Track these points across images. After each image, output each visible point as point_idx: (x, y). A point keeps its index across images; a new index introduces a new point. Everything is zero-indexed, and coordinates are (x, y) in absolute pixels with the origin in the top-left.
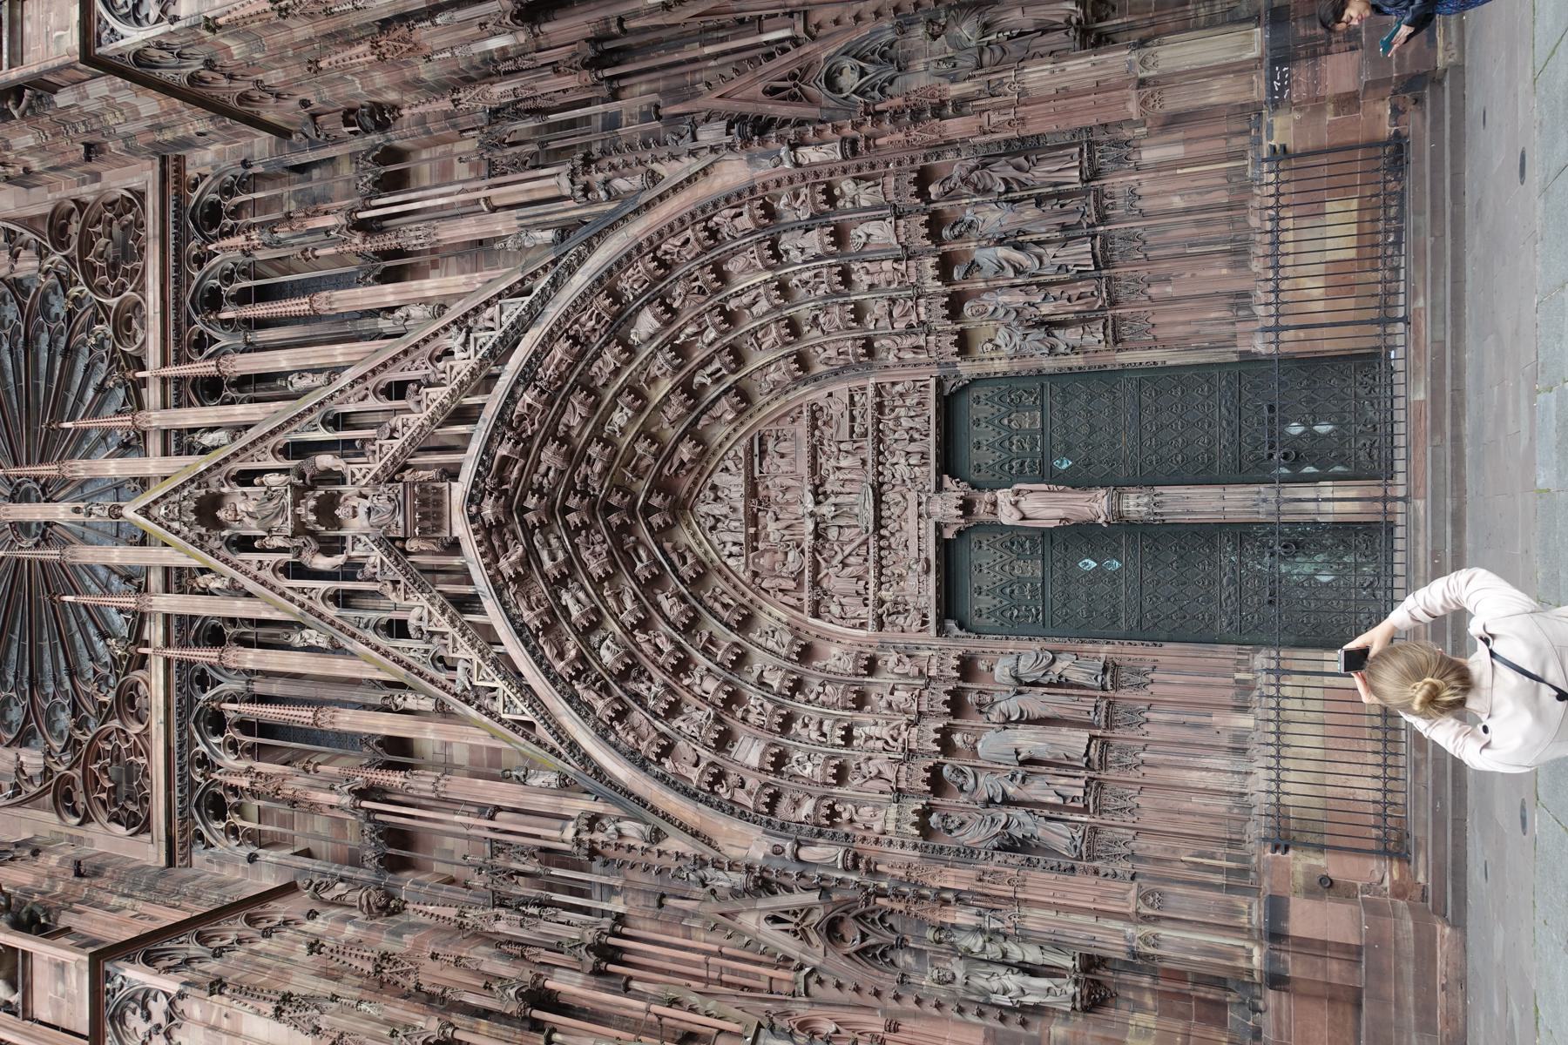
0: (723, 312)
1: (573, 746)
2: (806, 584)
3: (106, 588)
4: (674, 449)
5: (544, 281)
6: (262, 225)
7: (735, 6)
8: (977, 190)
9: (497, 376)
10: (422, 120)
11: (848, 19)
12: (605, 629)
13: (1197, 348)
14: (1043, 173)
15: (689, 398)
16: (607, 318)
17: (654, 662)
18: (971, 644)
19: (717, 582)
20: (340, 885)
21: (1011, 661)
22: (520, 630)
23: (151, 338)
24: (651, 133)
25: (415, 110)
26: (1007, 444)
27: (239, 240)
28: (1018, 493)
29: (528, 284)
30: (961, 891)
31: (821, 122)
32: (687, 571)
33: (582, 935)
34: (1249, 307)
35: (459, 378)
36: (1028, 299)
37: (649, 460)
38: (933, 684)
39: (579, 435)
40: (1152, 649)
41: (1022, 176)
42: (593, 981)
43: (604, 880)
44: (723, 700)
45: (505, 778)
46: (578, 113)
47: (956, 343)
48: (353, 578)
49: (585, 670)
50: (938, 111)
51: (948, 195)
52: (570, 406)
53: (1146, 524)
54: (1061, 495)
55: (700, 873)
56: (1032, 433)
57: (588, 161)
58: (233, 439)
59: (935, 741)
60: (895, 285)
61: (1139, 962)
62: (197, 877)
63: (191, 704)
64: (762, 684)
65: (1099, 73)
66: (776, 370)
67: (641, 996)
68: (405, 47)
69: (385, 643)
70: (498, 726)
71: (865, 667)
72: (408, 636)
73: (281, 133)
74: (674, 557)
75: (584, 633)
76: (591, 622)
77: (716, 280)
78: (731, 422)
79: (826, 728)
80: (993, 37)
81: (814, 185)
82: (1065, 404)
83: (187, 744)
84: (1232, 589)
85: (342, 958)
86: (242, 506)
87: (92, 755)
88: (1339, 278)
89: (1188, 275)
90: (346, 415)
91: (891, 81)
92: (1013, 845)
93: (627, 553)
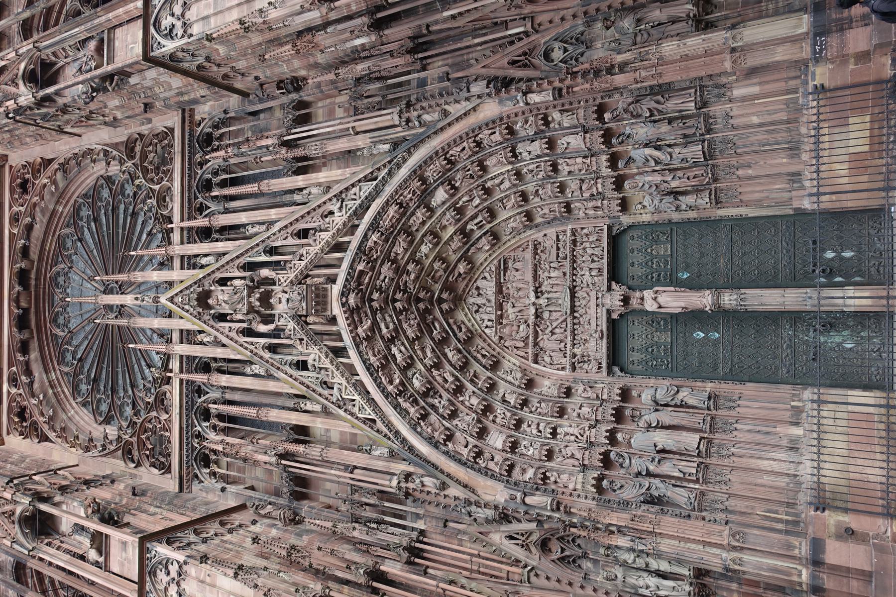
0: (484, 188)
1: (397, 433)
2: (531, 344)
3: (150, 341)
4: (456, 266)
5: (384, 172)
6: (233, 145)
7: (492, 15)
8: (633, 116)
9: (358, 226)
10: (319, 85)
11: (557, 20)
12: (416, 368)
13: (768, 206)
14: (672, 105)
15: (464, 238)
17: (443, 387)
18: (627, 381)
19: (479, 342)
20: (269, 507)
21: (652, 391)
22: (369, 367)
23: (176, 206)
24: (444, 88)
25: (315, 80)
26: (650, 263)
27: (222, 153)
28: (656, 292)
29: (375, 174)
30: (621, 526)
31: (541, 79)
32: (462, 336)
33: (401, 541)
34: (800, 181)
36: (663, 178)
37: (441, 272)
38: (605, 404)
39: (402, 258)
40: (739, 386)
41: (660, 107)
42: (406, 567)
43: (413, 510)
44: (482, 410)
45: (359, 450)
47: (619, 205)
48: (279, 337)
49: (404, 391)
50: (610, 71)
51: (615, 119)
53: (735, 311)
54: (683, 294)
55: (468, 508)
56: (665, 257)
57: (409, 105)
58: (217, 261)
59: (606, 437)
60: (583, 172)
61: (730, 574)
62: (194, 498)
63: (193, 404)
64: (504, 401)
65: (707, 45)
66: (514, 221)
67: (433, 578)
68: (310, 45)
69: (295, 373)
70: (356, 421)
71: (565, 393)
72: (307, 369)
73: (244, 94)
74: (455, 328)
75: (404, 370)
76: (408, 363)
77: (480, 170)
78: (488, 251)
79: (541, 428)
80: (643, 27)
81: (537, 115)
82: (685, 239)
83: (190, 426)
84: (789, 351)
85: (270, 547)
86: (221, 297)
87: (142, 430)
88: (858, 163)
89: (762, 163)
90: (276, 247)
91: (582, 54)
92: (652, 500)
93: (428, 325)
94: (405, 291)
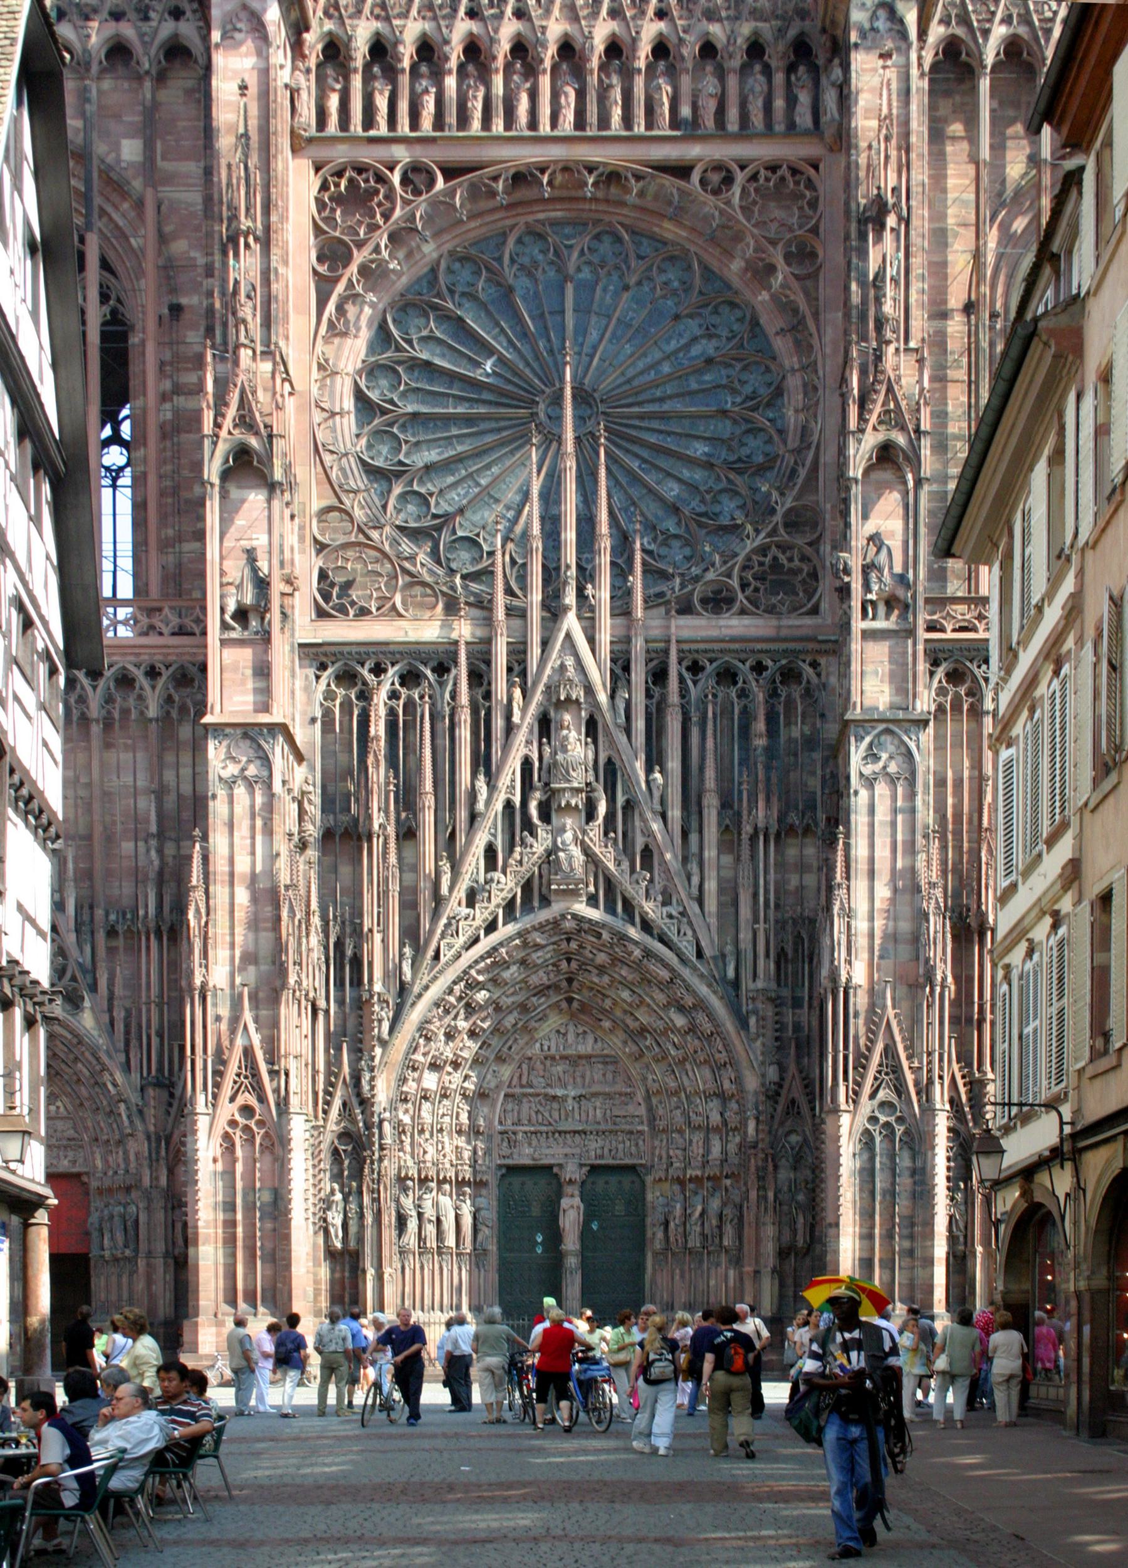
72: (487, 871)
75: (494, 981)
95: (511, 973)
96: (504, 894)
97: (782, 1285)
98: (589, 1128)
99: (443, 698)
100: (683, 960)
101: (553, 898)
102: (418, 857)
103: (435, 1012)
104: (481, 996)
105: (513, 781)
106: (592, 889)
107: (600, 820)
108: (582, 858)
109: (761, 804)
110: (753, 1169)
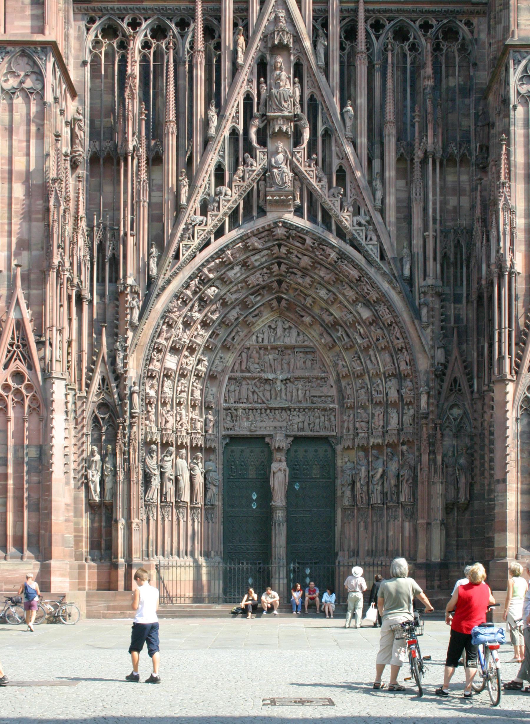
1: (169, 282)
16: (368, 297)
17: (208, 311)
35: (344, 220)
46: (465, 283)
48: (245, 152)
52: (329, 271)
72: (216, 186)
89: (366, 535)
94: (287, 273)
95: (235, 273)
96: (230, 204)
97: (447, 535)
98: (293, 406)
99: (184, 47)
100: (370, 261)
101: (268, 209)
102: (164, 176)
103: (175, 304)
104: (212, 291)
105: (237, 112)
106: (298, 201)
107: (305, 145)
108: (291, 174)
109: (430, 133)
110: (425, 436)
